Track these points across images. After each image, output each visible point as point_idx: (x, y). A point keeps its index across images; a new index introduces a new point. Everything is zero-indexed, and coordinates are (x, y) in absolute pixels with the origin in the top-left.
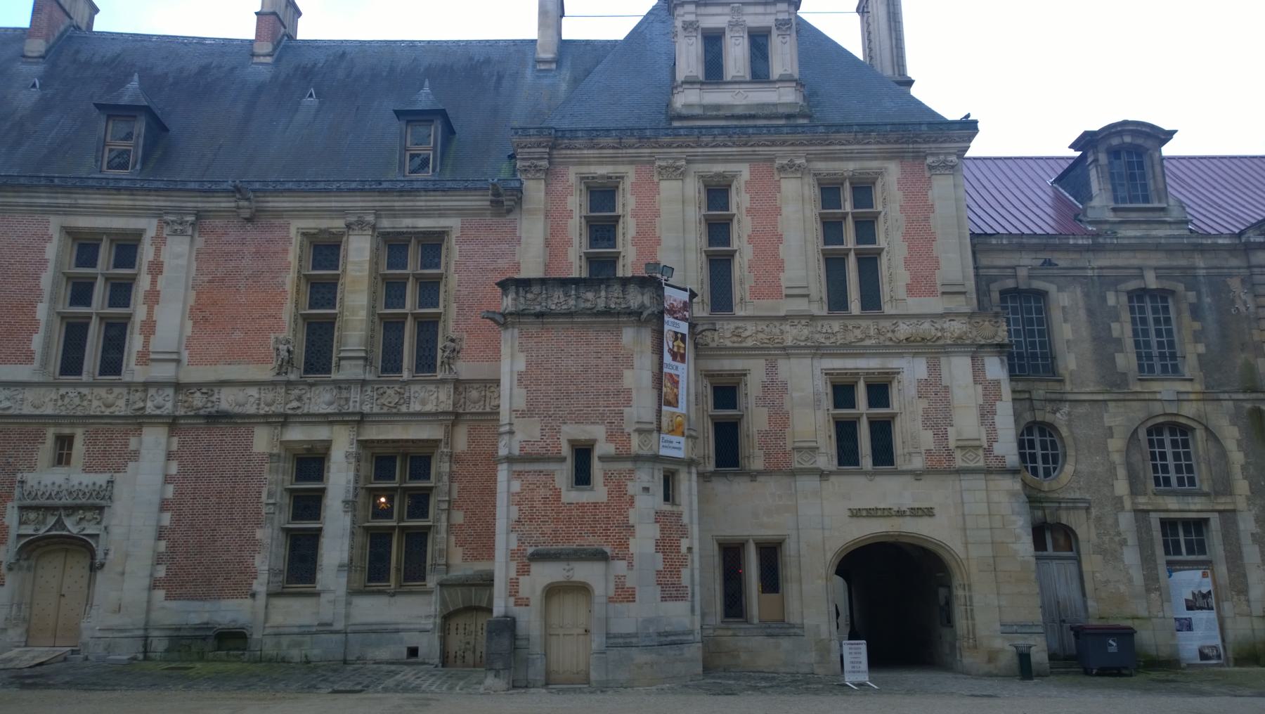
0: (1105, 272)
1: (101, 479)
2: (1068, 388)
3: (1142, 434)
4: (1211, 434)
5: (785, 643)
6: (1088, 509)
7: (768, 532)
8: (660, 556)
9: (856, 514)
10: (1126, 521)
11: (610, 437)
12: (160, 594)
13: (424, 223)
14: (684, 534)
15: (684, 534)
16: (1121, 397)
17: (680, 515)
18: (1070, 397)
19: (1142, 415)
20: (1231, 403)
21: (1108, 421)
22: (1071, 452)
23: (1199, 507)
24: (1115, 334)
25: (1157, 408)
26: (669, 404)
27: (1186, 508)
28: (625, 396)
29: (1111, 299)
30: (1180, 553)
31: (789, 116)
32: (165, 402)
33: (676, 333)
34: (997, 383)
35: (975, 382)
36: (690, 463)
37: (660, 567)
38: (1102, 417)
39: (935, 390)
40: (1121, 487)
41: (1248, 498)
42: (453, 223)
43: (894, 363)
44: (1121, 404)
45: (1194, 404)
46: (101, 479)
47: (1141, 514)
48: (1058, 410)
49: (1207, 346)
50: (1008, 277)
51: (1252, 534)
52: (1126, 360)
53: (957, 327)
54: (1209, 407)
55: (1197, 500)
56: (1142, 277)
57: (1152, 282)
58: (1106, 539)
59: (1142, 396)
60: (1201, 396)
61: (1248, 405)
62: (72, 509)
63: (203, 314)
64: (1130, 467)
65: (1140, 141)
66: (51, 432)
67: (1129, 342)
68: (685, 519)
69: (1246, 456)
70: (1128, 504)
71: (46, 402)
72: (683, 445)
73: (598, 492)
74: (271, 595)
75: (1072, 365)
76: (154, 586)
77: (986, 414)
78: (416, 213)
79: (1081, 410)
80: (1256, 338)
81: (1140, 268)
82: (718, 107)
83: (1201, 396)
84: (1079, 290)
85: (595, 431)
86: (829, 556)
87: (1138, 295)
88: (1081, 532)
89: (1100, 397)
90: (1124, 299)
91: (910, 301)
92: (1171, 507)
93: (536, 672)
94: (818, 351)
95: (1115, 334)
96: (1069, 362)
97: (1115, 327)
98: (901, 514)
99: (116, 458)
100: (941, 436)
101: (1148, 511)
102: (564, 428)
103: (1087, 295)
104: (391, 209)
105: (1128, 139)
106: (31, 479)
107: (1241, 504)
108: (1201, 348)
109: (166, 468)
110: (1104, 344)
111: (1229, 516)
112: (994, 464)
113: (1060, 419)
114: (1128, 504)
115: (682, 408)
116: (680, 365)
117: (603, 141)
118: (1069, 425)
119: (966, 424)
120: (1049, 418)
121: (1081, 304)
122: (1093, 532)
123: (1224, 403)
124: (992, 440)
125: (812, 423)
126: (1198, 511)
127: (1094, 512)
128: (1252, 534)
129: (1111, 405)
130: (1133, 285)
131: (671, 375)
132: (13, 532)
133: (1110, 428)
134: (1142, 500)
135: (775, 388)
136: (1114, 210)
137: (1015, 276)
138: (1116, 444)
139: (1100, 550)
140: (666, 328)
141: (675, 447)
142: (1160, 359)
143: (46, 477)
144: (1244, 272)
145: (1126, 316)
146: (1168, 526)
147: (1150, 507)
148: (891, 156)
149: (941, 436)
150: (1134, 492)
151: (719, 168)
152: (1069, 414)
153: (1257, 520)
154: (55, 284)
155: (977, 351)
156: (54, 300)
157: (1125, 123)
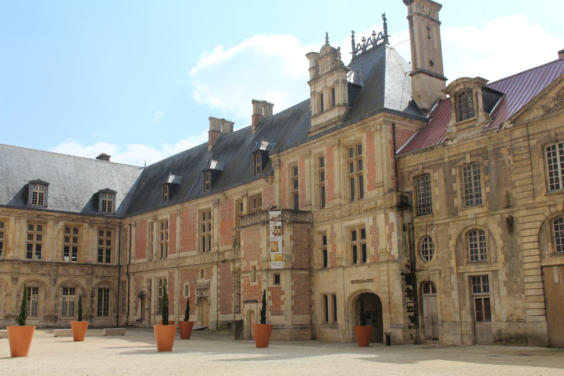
0: (452, 159)
1: (208, 281)
2: (435, 218)
3: (463, 235)
4: (490, 233)
5: (335, 331)
6: (440, 274)
7: (332, 291)
8: (271, 301)
9: (353, 282)
10: (454, 277)
11: (259, 264)
12: (219, 312)
13: (257, 192)
14: (283, 293)
15: (283, 293)
16: (454, 220)
17: (281, 288)
18: (435, 223)
19: (462, 227)
20: (499, 215)
21: (450, 232)
22: (435, 248)
23: (483, 269)
24: (454, 189)
25: (468, 223)
26: (273, 251)
27: (478, 270)
28: (260, 250)
29: (454, 172)
30: (479, 291)
31: (335, 123)
32: (216, 259)
33: (276, 227)
34: (393, 223)
35: (386, 224)
36: (285, 269)
37: (271, 305)
38: (447, 231)
39: (375, 228)
40: (453, 263)
41: (503, 264)
42: (261, 190)
43: (364, 220)
44: (455, 223)
45: (483, 219)
46: (208, 281)
47: (460, 275)
48: (432, 229)
49: (491, 188)
50: (416, 170)
51: (504, 282)
52: (458, 201)
53: (379, 202)
54: (490, 219)
55: (483, 266)
56: (464, 158)
57: (468, 160)
58: (446, 287)
59: (462, 218)
60: (486, 214)
61: (506, 216)
62: (204, 289)
63: (222, 231)
64: (456, 252)
65: (467, 86)
66: (200, 268)
67: (459, 192)
68: (283, 289)
69: (504, 242)
70: (455, 271)
71: (198, 261)
72: (282, 264)
73: (256, 283)
74: (235, 313)
75: (438, 208)
76: (217, 311)
77: (389, 237)
78: (254, 189)
79: (440, 228)
80: (513, 179)
81: (464, 153)
82: (318, 125)
83: (486, 214)
84: (441, 170)
85: (255, 263)
86: (346, 299)
87: (467, 167)
88: (437, 285)
89: (446, 221)
90: (458, 171)
91: (368, 193)
92: (471, 270)
93: (245, 335)
94: (342, 218)
95: (454, 189)
96: (438, 205)
97: (454, 185)
98: (364, 281)
99: (210, 276)
100: (376, 249)
101: (463, 273)
102: (250, 262)
103: (444, 172)
104: (248, 189)
105: (462, 87)
106: (198, 281)
107: (500, 266)
108: (488, 189)
109: (218, 277)
110: (450, 194)
111: (495, 272)
112: (391, 258)
113: (432, 234)
114: (455, 271)
115: (280, 251)
116: (279, 237)
117: (290, 150)
118: (436, 237)
119: (383, 244)
120: (428, 233)
121: (442, 177)
122: (442, 284)
123: (496, 216)
124: (391, 249)
125: (340, 247)
126: (484, 271)
127: (443, 275)
128: (504, 282)
129: (451, 224)
130: (461, 163)
131: (274, 242)
133: (450, 235)
134: (462, 268)
135: (333, 235)
136: (456, 126)
137: (418, 169)
138: (452, 242)
139: (445, 293)
140: (271, 226)
141: (280, 265)
142: (471, 198)
143: (201, 281)
144: (509, 143)
145: (458, 179)
146: (474, 280)
147: (464, 271)
148: (364, 130)
149: (376, 249)
150: (458, 265)
151: (319, 150)
152: (436, 231)
153: (506, 274)
154: (199, 227)
155: (385, 209)
156: (199, 232)
157: (457, 80)
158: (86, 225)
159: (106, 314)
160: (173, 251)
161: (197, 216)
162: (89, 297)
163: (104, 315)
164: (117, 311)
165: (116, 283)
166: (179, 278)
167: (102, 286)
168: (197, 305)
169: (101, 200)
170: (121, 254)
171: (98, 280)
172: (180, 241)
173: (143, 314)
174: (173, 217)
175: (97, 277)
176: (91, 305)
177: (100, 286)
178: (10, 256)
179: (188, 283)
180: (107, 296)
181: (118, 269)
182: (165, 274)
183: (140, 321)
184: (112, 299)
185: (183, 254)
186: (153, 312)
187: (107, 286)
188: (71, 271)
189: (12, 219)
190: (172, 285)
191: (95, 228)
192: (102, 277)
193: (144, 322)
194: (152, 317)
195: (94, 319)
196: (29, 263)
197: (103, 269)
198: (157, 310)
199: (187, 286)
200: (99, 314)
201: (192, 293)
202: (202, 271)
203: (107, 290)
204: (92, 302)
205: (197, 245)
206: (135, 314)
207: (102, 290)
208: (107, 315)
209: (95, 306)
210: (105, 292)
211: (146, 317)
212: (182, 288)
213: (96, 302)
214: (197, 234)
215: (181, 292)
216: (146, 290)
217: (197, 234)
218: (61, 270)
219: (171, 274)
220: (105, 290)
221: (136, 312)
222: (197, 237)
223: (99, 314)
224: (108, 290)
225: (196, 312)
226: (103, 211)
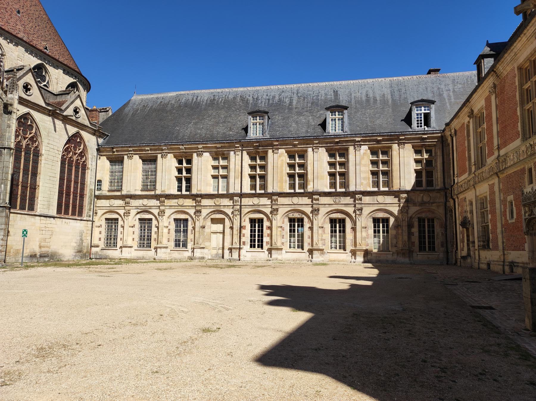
132: (523, 217)
158: (395, 146)
159: (432, 249)
160: (491, 154)
161: (517, 79)
162: (405, 229)
163: (429, 249)
164: (445, 245)
165: (441, 211)
166: (500, 190)
167: (423, 215)
168: (527, 233)
169: (415, 112)
170: (446, 174)
171: (417, 208)
172: (498, 132)
173: (469, 249)
174: (488, 100)
175: (415, 204)
176: (409, 238)
177: (419, 216)
178: (310, 188)
179: (511, 198)
180: (432, 227)
181: (443, 193)
182: (483, 189)
183: (463, 258)
184: (438, 230)
185: (502, 152)
186: (476, 247)
187: (430, 216)
188: (380, 198)
189: (310, 150)
190: (493, 202)
191: (409, 147)
192: (422, 203)
193: (469, 260)
194: (477, 252)
195: (415, 255)
197: (422, 195)
198: (482, 243)
199: (511, 203)
200: (422, 248)
201: (519, 214)
202: (530, 170)
203: (431, 221)
204: (410, 234)
205: (520, 129)
206: (462, 250)
207: (424, 220)
208: (434, 249)
209: (415, 239)
210: (428, 222)
211: (472, 253)
212: (505, 205)
213: (416, 234)
214: (518, 109)
215: (504, 214)
216: (469, 215)
217: (518, 109)
218: (366, 199)
219: (492, 187)
220: (429, 220)
221: (463, 246)
222: (519, 114)
223: (422, 248)
224: (433, 220)
225: (526, 246)
226: (418, 127)
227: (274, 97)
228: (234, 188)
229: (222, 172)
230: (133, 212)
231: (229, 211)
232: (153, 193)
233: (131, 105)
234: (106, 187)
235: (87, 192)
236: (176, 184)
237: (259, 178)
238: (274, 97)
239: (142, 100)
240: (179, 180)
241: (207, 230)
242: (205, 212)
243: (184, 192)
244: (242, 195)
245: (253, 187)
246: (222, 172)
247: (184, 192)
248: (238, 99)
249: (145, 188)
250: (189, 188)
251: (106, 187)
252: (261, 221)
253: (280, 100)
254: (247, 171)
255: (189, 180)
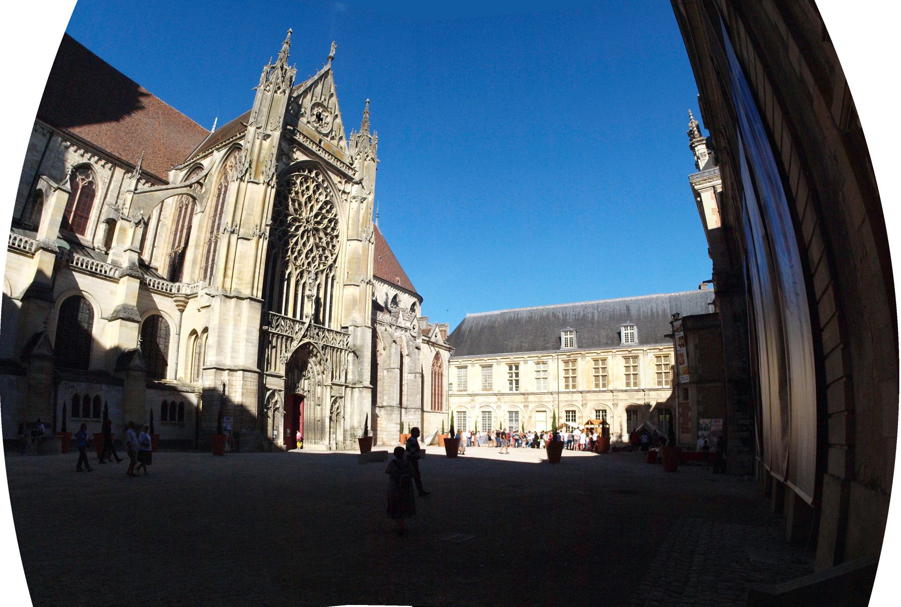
178: (611, 387)
196: (626, 391)
227: (579, 313)
228: (553, 387)
229: (542, 375)
230: (478, 406)
231: (549, 405)
232: (491, 392)
233: (466, 323)
234: (455, 387)
235: (444, 393)
236: (508, 386)
237: (571, 379)
238: (579, 313)
239: (474, 318)
240: (511, 384)
241: (533, 419)
242: (531, 406)
243: (514, 391)
244: (558, 393)
245: (567, 387)
246: (542, 375)
247: (514, 391)
248: (551, 315)
249: (485, 389)
250: (517, 387)
251: (455, 387)
252: (574, 412)
253: (584, 316)
254: (562, 374)
255: (517, 382)
